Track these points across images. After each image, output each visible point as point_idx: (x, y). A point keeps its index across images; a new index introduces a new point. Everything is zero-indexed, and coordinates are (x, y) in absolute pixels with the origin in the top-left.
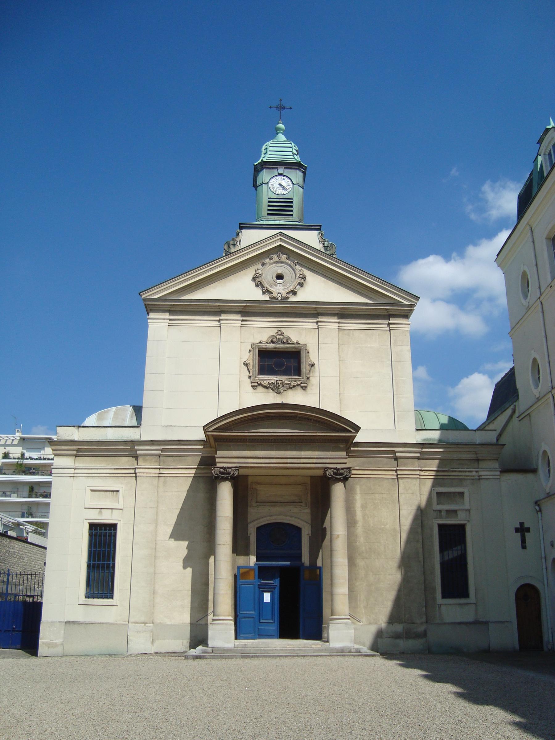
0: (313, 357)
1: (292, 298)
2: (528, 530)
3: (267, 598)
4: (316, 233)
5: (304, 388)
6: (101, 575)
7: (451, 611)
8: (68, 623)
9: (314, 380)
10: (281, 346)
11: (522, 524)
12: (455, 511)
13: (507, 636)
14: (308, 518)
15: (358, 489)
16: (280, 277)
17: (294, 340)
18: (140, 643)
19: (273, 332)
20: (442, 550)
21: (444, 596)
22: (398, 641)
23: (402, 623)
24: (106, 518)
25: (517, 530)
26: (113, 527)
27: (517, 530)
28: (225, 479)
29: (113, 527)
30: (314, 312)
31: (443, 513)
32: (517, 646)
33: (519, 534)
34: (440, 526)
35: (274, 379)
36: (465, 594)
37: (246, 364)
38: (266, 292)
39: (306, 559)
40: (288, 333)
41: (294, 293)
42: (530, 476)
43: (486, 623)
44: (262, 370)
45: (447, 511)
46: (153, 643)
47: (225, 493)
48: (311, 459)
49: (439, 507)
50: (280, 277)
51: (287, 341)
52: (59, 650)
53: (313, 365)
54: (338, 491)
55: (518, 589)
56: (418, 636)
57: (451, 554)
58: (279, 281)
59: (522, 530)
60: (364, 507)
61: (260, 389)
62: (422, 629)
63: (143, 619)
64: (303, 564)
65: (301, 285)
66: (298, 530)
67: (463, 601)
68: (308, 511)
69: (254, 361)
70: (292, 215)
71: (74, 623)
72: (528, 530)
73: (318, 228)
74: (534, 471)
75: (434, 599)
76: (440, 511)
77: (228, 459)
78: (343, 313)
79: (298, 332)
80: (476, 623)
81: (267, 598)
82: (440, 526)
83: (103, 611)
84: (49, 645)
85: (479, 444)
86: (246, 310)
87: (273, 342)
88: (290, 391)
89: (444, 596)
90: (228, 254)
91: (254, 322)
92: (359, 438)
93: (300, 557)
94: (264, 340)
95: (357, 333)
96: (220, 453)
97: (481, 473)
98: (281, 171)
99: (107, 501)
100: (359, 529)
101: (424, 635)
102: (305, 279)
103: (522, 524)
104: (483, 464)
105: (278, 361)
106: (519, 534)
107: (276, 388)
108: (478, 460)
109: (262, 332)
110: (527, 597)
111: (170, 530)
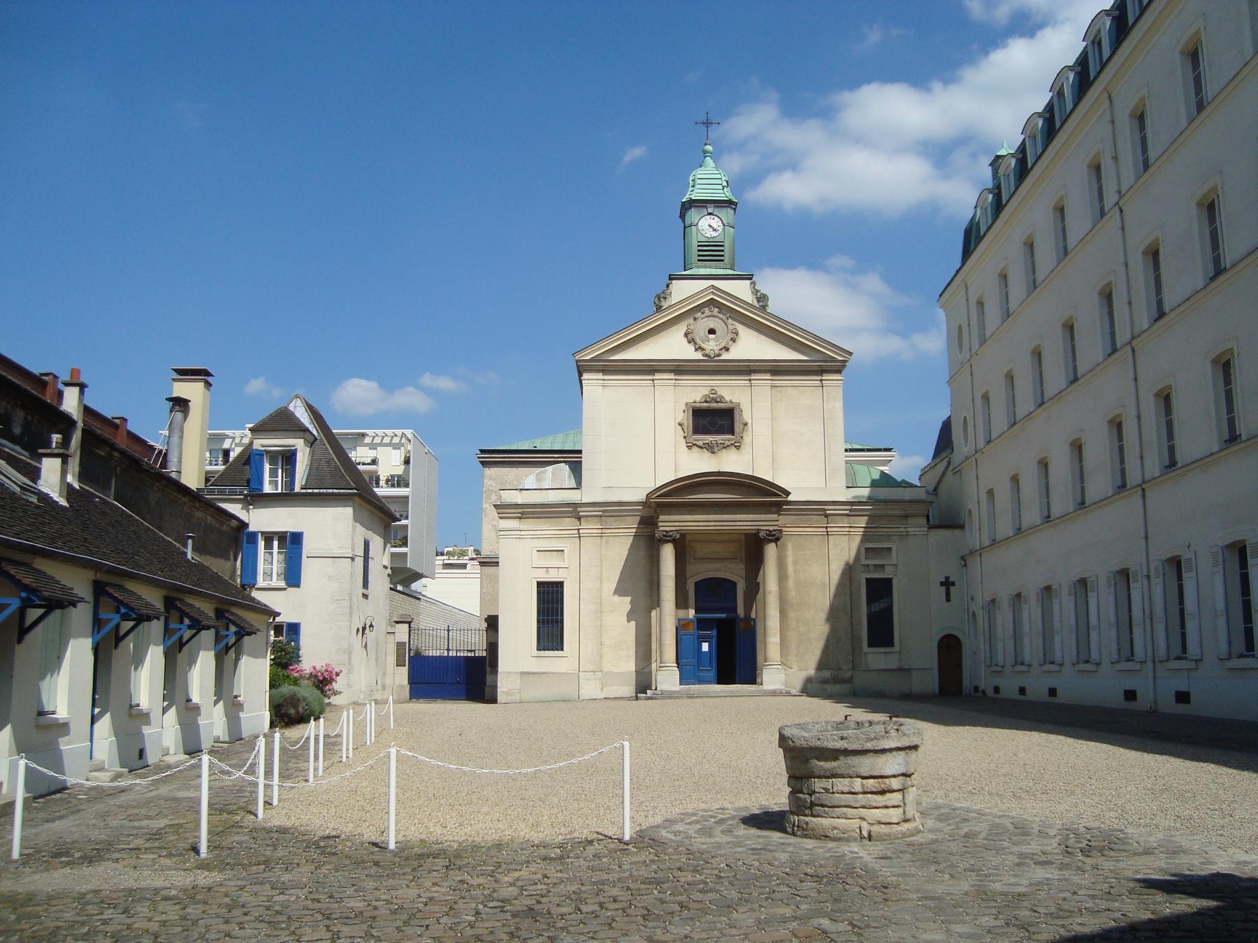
0: (746, 416)
1: (725, 356)
2: (953, 584)
3: (705, 647)
4: (748, 282)
5: (738, 448)
6: (550, 628)
7: (877, 659)
8: (522, 673)
9: (747, 439)
10: (714, 405)
11: (947, 578)
12: (883, 566)
13: (930, 682)
14: (743, 573)
15: (790, 546)
16: (712, 331)
18: (590, 689)
19: (706, 391)
20: (869, 602)
21: (870, 645)
24: (552, 577)
25: (942, 584)
26: (561, 584)
27: (942, 584)
28: (668, 541)
29: (561, 584)
30: (747, 369)
32: (937, 691)
33: (943, 588)
34: (868, 580)
35: (709, 438)
36: (891, 644)
39: (741, 612)
41: (727, 349)
42: (957, 532)
43: (909, 670)
44: (698, 429)
47: (668, 554)
49: (868, 562)
50: (712, 331)
51: (720, 400)
52: (517, 697)
53: (746, 424)
54: (771, 550)
57: (877, 607)
58: (712, 336)
59: (947, 584)
60: (795, 563)
61: (695, 448)
62: (849, 674)
63: (592, 668)
65: (734, 340)
66: (734, 584)
67: (888, 650)
68: (742, 566)
69: (688, 421)
71: (529, 673)
72: (953, 584)
73: (749, 277)
74: (962, 527)
75: (860, 648)
77: (669, 523)
78: (776, 369)
79: (731, 391)
80: (900, 669)
81: (705, 647)
82: (868, 580)
83: (553, 662)
84: (507, 693)
86: (680, 368)
89: (870, 645)
90: (659, 308)
91: (687, 380)
92: (790, 498)
93: (735, 609)
94: (698, 399)
95: (789, 390)
96: (662, 518)
98: (710, 210)
99: (553, 561)
100: (791, 583)
101: (850, 680)
103: (947, 578)
104: (911, 521)
105: (713, 421)
106: (943, 588)
107: (710, 448)
108: (906, 517)
109: (696, 391)
110: (950, 647)
111: (613, 586)
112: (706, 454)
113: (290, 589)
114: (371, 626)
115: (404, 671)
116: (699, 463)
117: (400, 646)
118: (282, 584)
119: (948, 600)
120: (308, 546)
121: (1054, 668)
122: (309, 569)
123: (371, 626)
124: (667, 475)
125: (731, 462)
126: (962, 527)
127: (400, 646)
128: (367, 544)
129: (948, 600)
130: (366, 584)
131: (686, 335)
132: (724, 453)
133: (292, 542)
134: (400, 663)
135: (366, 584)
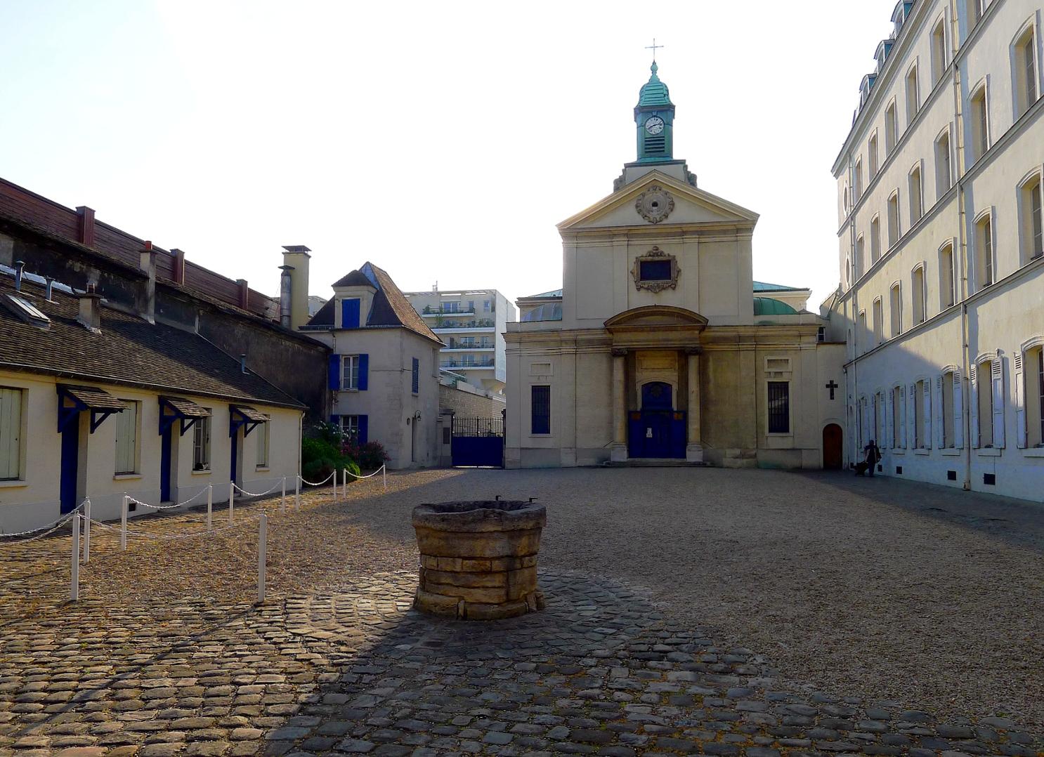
0: (680, 265)
1: (665, 222)
2: (836, 386)
5: (674, 289)
7: (776, 441)
8: (522, 449)
9: (680, 282)
10: (656, 259)
11: (831, 382)
13: (817, 459)
14: (676, 379)
15: (711, 359)
16: (655, 204)
17: (666, 253)
18: (568, 460)
19: (650, 248)
20: (770, 400)
21: (771, 431)
22: (737, 460)
23: (740, 448)
25: (827, 386)
27: (827, 386)
28: (620, 356)
30: (682, 232)
31: (772, 375)
32: (822, 466)
33: (829, 389)
35: (651, 283)
36: (787, 431)
37: (632, 272)
38: (645, 217)
40: (662, 249)
41: (666, 217)
42: (841, 347)
45: (775, 373)
46: (576, 461)
48: (678, 337)
49: (769, 370)
50: (655, 204)
51: (662, 254)
55: (829, 425)
56: (751, 457)
57: (776, 403)
58: (655, 208)
59: (832, 386)
62: (754, 452)
64: (672, 410)
67: (784, 434)
68: (676, 374)
69: (637, 270)
70: (663, 151)
71: (526, 449)
72: (836, 386)
74: (845, 343)
75: (763, 433)
76: (770, 373)
79: (669, 248)
80: (793, 449)
83: (544, 441)
85: (802, 325)
86: (630, 233)
87: (650, 256)
88: (663, 291)
89: (771, 431)
97: (801, 346)
98: (654, 114)
100: (711, 386)
102: (673, 205)
103: (831, 382)
105: (656, 270)
106: (829, 389)
109: (642, 249)
110: (833, 434)
112: (650, 294)
113: (361, 392)
114: (419, 417)
115: (449, 446)
116: (644, 299)
117: (446, 430)
118: (356, 390)
119: (832, 398)
120: (372, 364)
121: (901, 451)
122: (374, 378)
123: (419, 417)
124: (621, 308)
125: (669, 299)
126: (845, 343)
127: (446, 430)
128: (415, 362)
129: (832, 398)
130: (415, 389)
131: (637, 207)
132: (664, 292)
133: (363, 360)
134: (445, 442)
135: (415, 389)
